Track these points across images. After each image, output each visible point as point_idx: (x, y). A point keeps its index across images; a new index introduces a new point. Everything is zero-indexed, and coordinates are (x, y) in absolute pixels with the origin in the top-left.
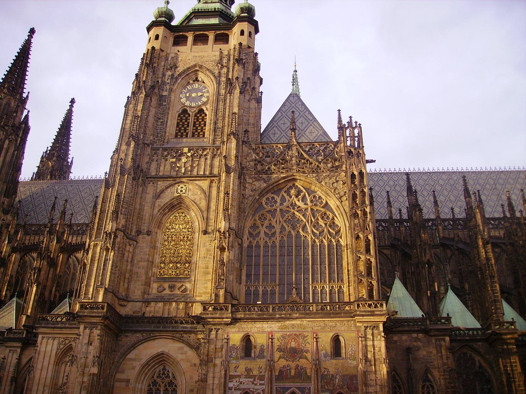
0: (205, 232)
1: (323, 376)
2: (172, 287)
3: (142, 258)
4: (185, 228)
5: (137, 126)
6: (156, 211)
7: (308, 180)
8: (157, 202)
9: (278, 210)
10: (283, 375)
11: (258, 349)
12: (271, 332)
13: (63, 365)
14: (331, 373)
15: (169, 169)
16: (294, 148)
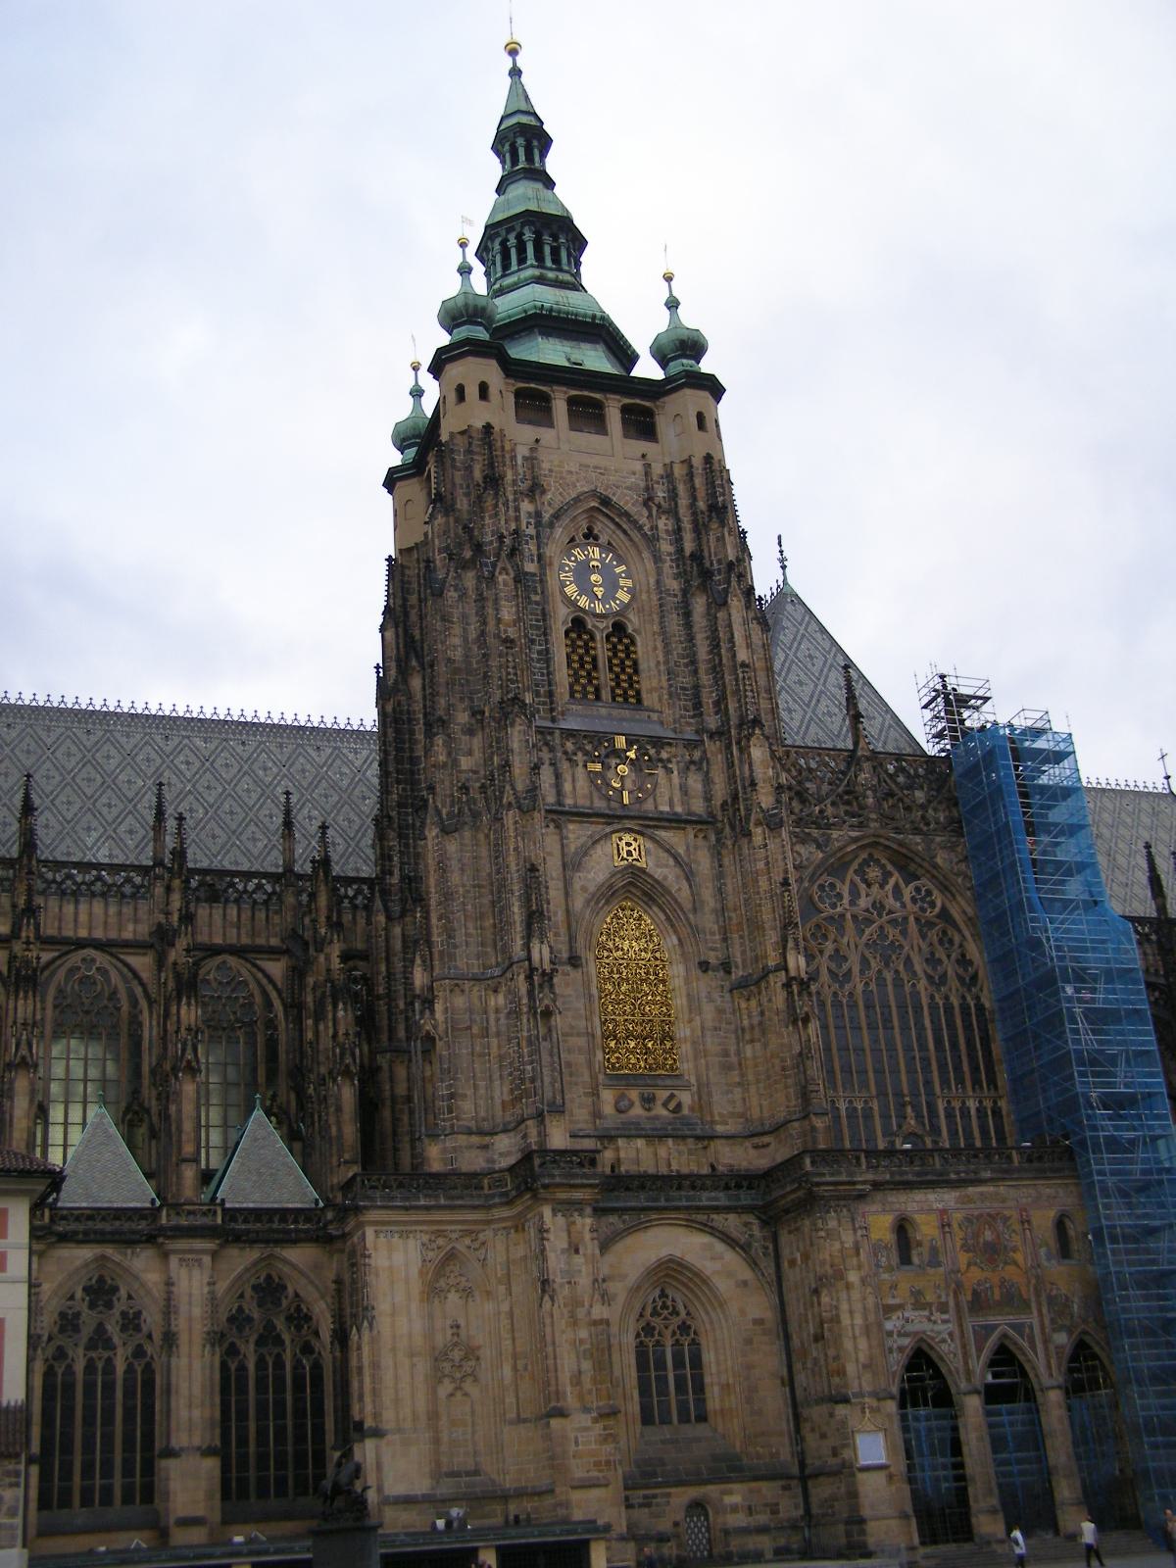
0: (704, 966)
1: (1051, 1300)
2: (648, 1101)
3: (572, 1027)
4: (645, 950)
5: (514, 668)
6: (578, 903)
7: (904, 851)
8: (576, 879)
9: (848, 916)
10: (979, 1303)
11: (925, 1250)
12: (943, 1212)
13: (436, 1301)
14: (1064, 1291)
15: (586, 791)
16: (866, 765)
